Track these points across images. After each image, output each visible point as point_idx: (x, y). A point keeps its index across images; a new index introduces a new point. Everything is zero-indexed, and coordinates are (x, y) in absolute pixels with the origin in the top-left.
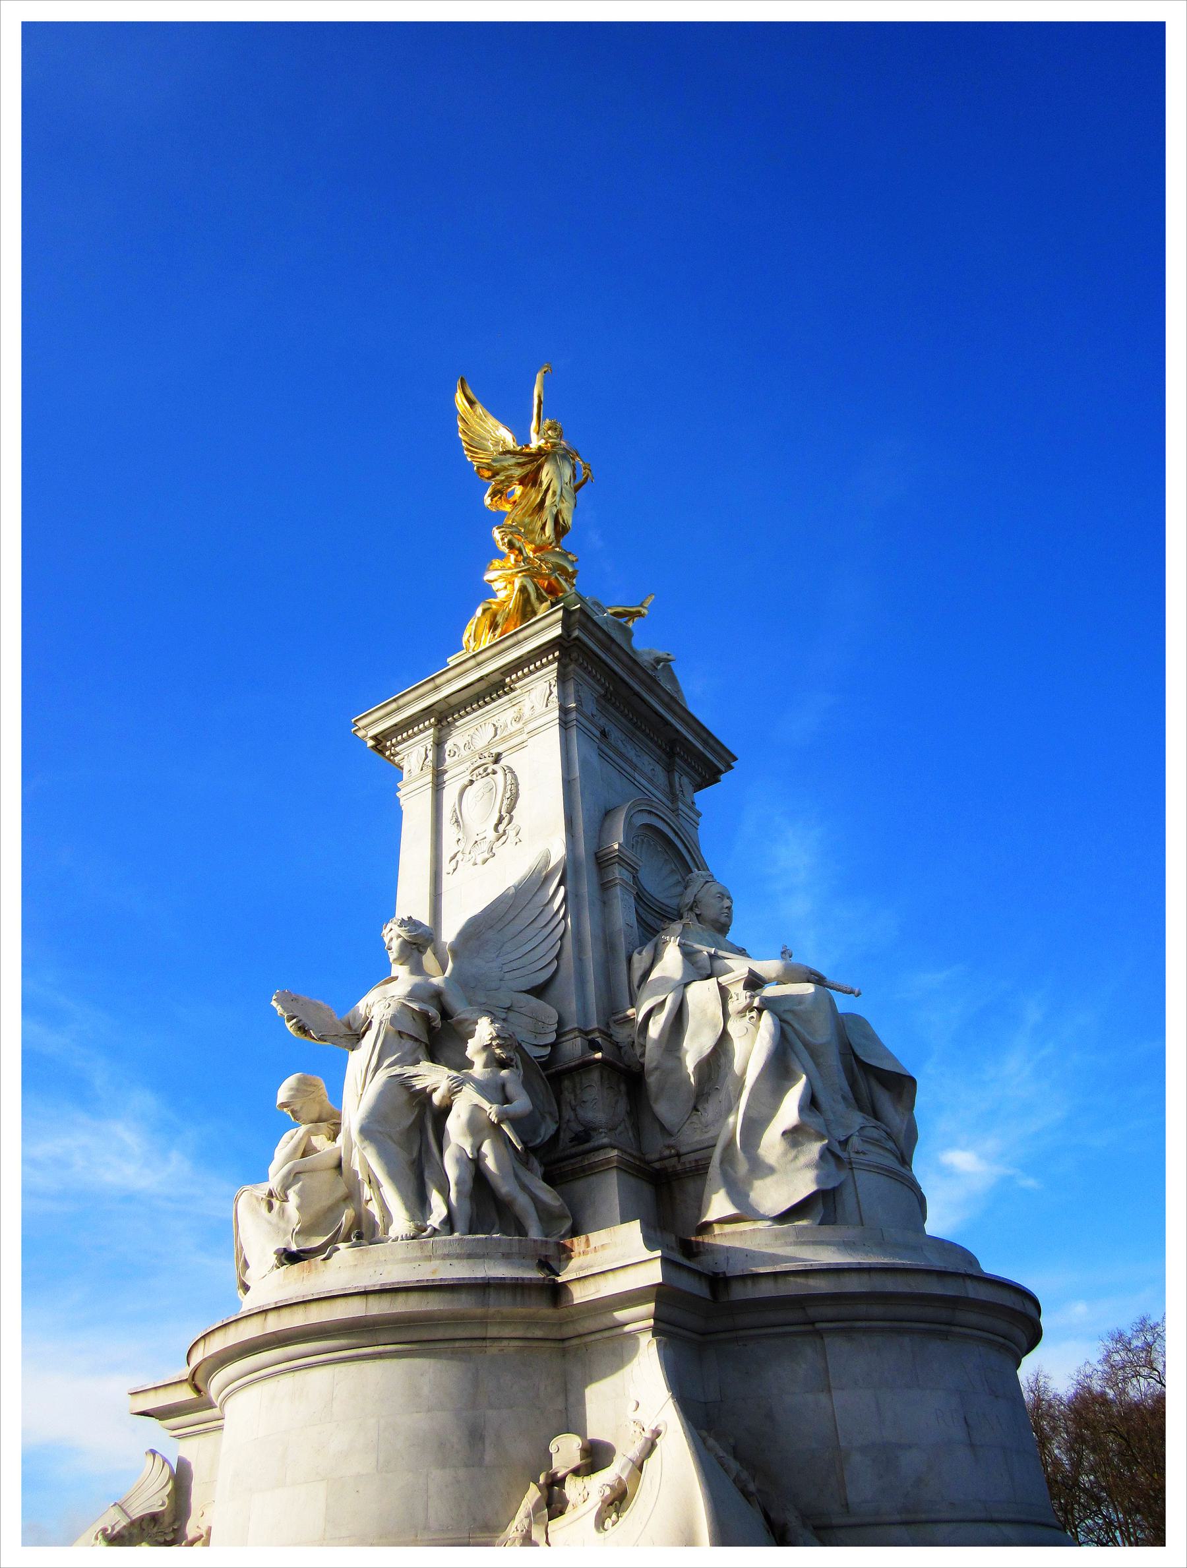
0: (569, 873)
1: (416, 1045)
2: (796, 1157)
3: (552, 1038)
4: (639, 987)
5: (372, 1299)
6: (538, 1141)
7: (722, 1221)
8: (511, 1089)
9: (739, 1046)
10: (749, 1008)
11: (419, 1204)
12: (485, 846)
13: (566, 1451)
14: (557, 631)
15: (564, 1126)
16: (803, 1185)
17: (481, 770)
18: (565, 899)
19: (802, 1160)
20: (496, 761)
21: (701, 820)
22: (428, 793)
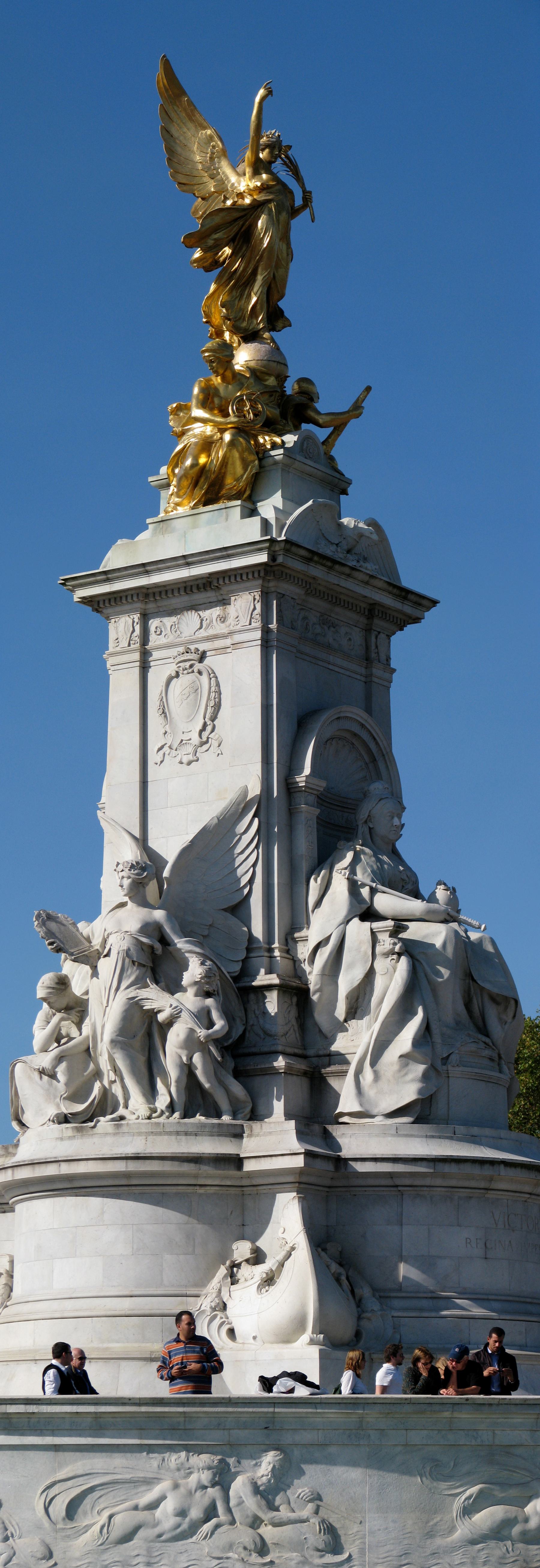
0: (262, 805)
1: (144, 970)
2: (406, 1074)
3: (243, 955)
4: (313, 911)
5: (130, 1162)
6: (231, 1041)
7: (351, 1114)
8: (215, 1015)
9: (379, 982)
10: (392, 952)
11: (151, 1093)
12: (190, 749)
13: (242, 1250)
14: (263, 558)
15: (249, 1028)
16: (409, 1093)
17: (188, 664)
18: (258, 831)
19: (410, 1076)
20: (202, 659)
21: (395, 675)
22: (136, 672)
